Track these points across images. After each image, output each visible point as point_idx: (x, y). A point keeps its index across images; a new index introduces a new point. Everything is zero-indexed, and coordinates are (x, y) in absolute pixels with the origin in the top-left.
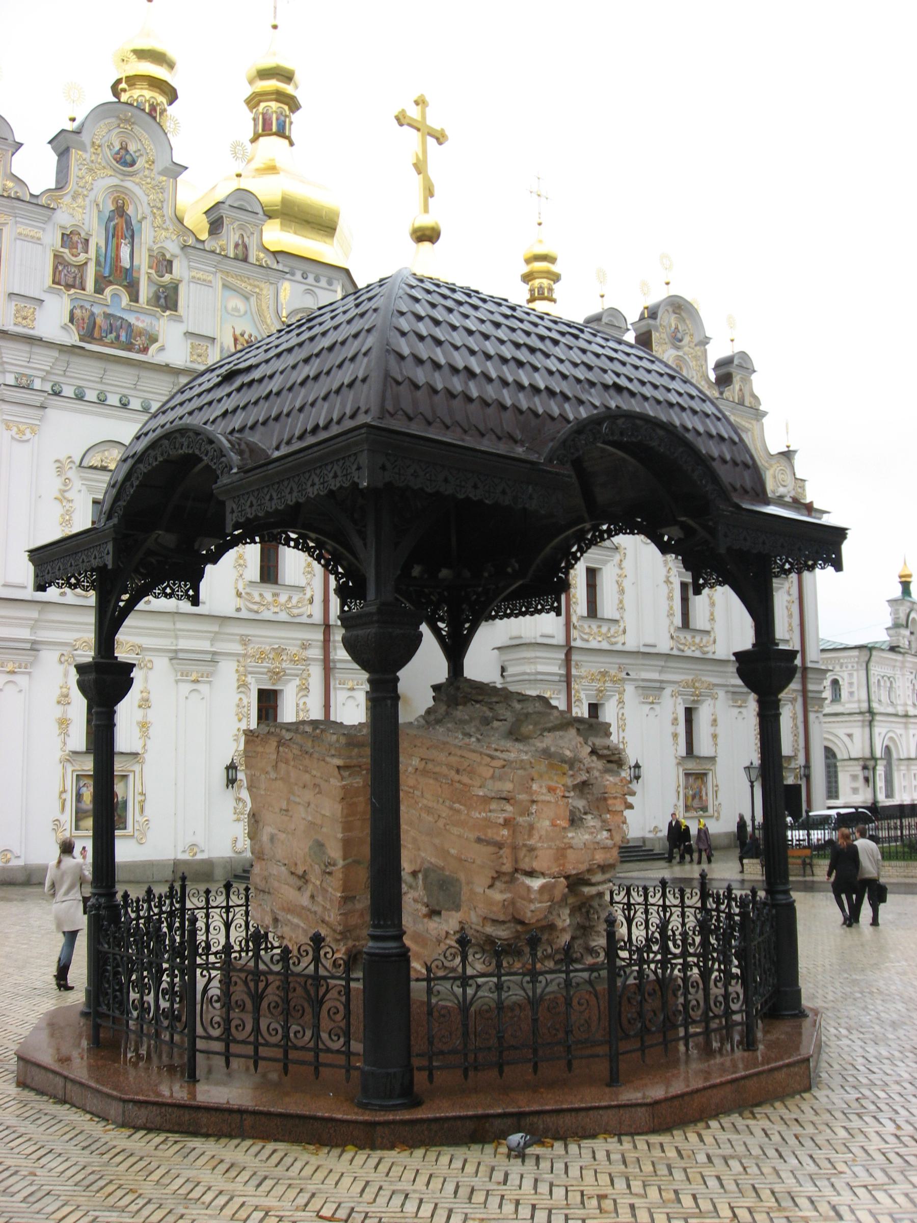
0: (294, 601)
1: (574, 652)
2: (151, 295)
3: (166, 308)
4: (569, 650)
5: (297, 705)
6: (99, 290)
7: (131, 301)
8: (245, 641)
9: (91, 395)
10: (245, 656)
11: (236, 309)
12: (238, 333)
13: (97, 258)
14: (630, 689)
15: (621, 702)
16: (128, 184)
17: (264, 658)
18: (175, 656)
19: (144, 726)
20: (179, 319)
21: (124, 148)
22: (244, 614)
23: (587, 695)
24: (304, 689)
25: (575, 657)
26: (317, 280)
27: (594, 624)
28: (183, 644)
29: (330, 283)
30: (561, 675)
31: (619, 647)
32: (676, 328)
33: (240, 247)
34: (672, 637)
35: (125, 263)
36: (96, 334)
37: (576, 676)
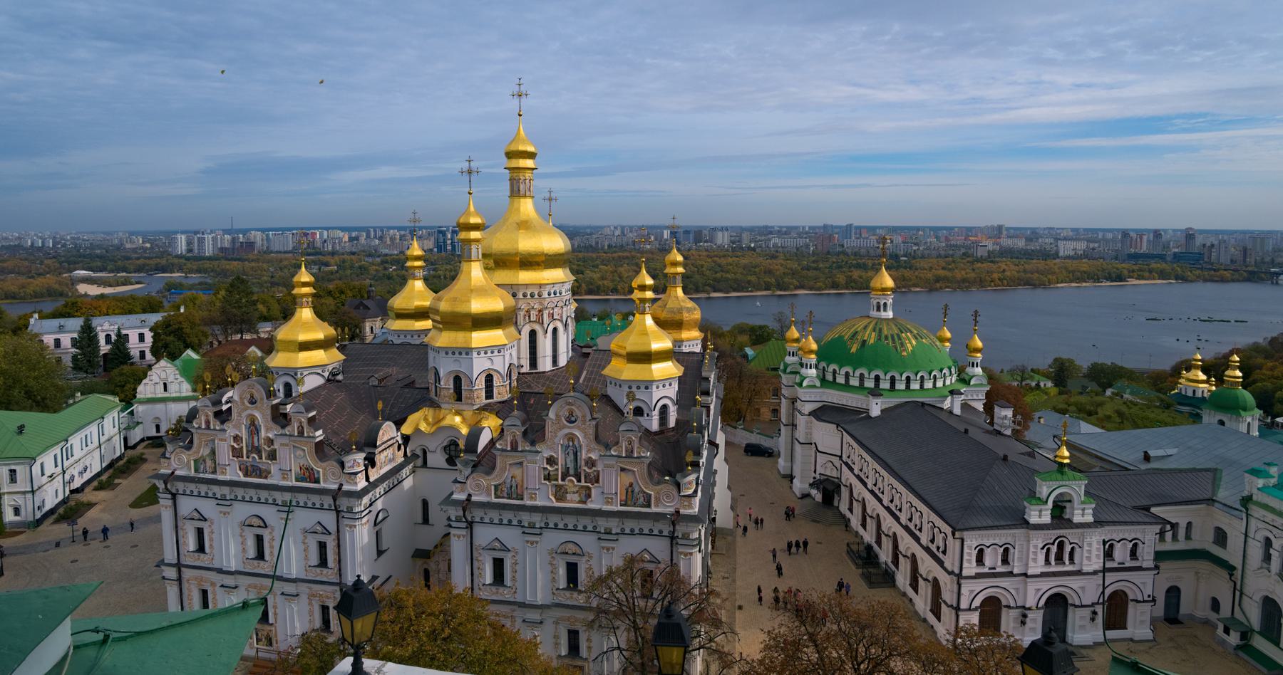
6: (248, 457)
26: (460, 353)
29: (467, 354)
32: (571, 414)
34: (553, 594)
35: (256, 444)
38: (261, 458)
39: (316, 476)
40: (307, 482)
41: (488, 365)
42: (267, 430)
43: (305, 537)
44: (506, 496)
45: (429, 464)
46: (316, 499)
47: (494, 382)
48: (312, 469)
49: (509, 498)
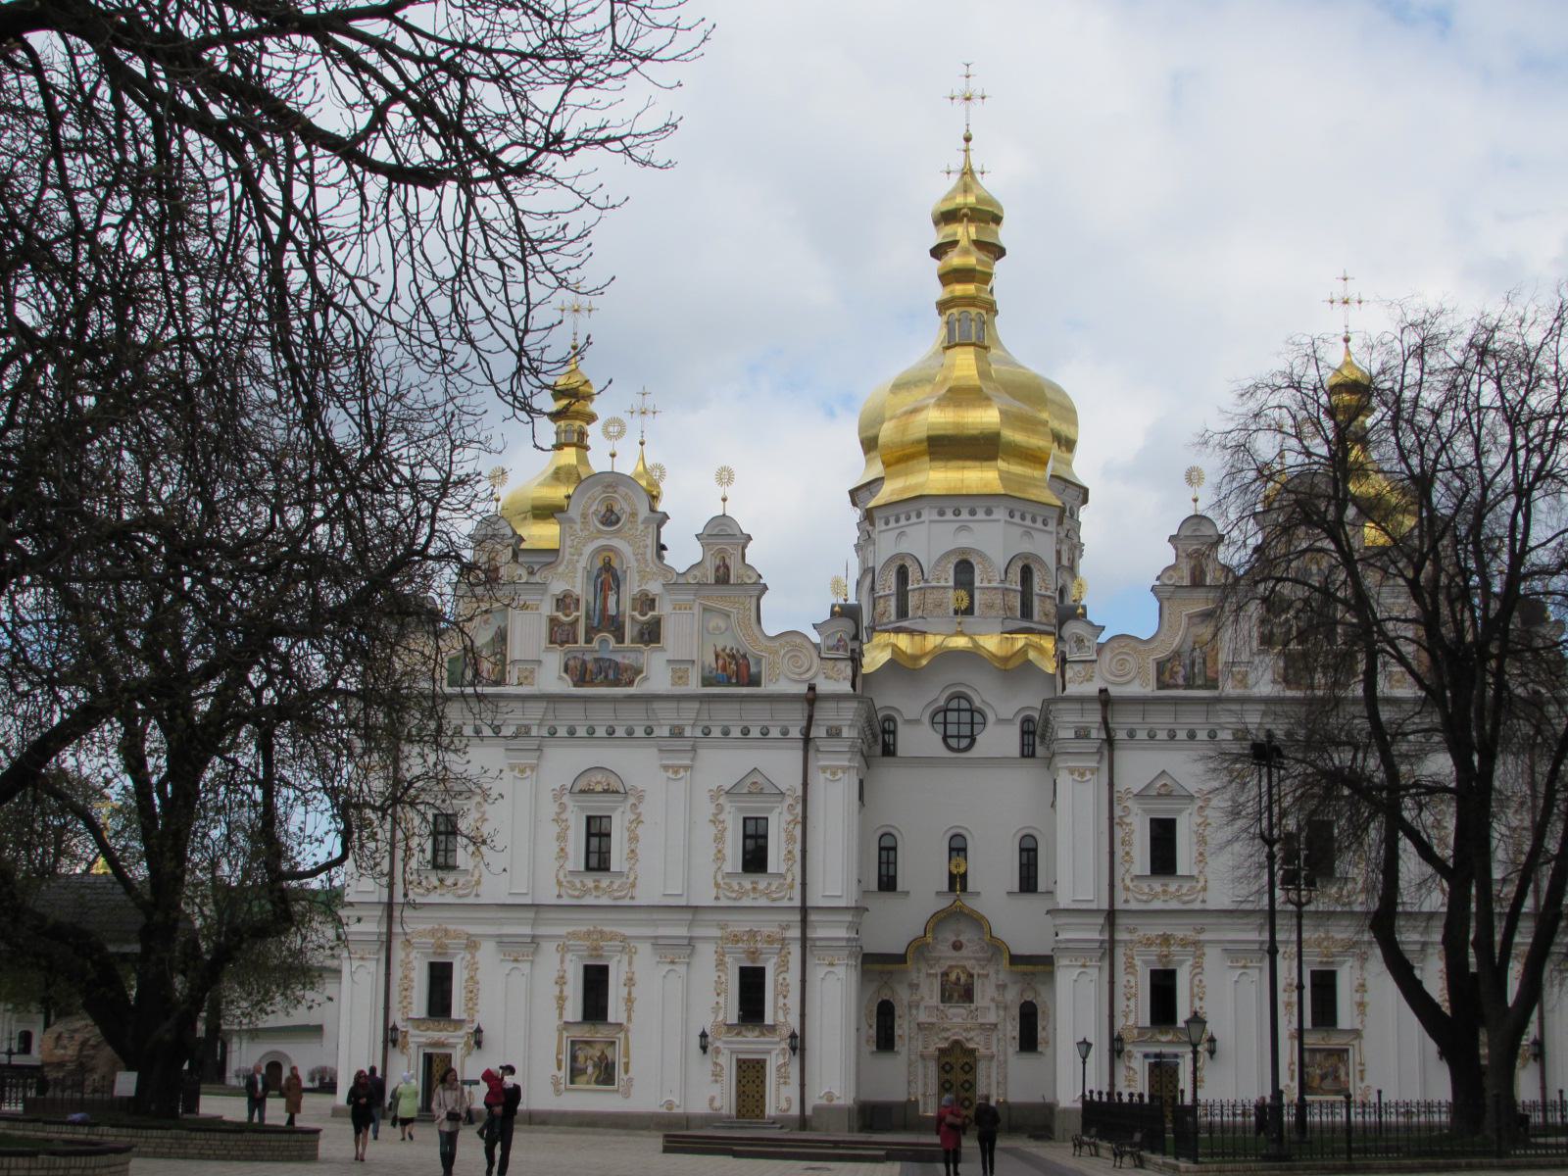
0: (773, 888)
1: (1117, 914)
2: (635, 633)
3: (651, 641)
4: (1111, 915)
5: (776, 981)
6: (588, 641)
7: (618, 642)
8: (722, 927)
9: (581, 732)
10: (721, 938)
11: (718, 628)
12: (719, 649)
13: (587, 613)
14: (1212, 955)
15: (1198, 967)
16: (616, 543)
17: (737, 942)
18: (656, 942)
19: (629, 1001)
20: (662, 649)
21: (610, 510)
22: (724, 902)
23: (1145, 962)
24: (783, 966)
25: (1121, 921)
26: (973, 513)
27: (1157, 885)
28: (662, 931)
29: (989, 512)
30: (1102, 942)
31: (1197, 906)
33: (722, 570)
35: (612, 610)
36: (587, 678)
37: (1131, 941)
38: (620, 639)
39: (753, 670)
40: (729, 684)
41: (1026, 547)
42: (643, 576)
43: (720, 808)
44: (1180, 681)
45: (903, 749)
46: (756, 717)
47: (1036, 589)
48: (744, 656)
49: (1189, 686)
